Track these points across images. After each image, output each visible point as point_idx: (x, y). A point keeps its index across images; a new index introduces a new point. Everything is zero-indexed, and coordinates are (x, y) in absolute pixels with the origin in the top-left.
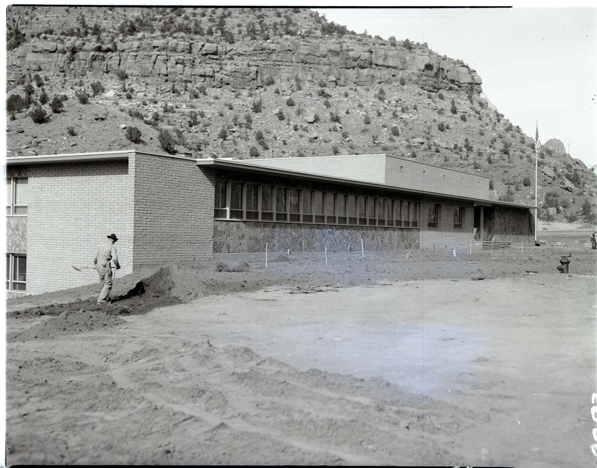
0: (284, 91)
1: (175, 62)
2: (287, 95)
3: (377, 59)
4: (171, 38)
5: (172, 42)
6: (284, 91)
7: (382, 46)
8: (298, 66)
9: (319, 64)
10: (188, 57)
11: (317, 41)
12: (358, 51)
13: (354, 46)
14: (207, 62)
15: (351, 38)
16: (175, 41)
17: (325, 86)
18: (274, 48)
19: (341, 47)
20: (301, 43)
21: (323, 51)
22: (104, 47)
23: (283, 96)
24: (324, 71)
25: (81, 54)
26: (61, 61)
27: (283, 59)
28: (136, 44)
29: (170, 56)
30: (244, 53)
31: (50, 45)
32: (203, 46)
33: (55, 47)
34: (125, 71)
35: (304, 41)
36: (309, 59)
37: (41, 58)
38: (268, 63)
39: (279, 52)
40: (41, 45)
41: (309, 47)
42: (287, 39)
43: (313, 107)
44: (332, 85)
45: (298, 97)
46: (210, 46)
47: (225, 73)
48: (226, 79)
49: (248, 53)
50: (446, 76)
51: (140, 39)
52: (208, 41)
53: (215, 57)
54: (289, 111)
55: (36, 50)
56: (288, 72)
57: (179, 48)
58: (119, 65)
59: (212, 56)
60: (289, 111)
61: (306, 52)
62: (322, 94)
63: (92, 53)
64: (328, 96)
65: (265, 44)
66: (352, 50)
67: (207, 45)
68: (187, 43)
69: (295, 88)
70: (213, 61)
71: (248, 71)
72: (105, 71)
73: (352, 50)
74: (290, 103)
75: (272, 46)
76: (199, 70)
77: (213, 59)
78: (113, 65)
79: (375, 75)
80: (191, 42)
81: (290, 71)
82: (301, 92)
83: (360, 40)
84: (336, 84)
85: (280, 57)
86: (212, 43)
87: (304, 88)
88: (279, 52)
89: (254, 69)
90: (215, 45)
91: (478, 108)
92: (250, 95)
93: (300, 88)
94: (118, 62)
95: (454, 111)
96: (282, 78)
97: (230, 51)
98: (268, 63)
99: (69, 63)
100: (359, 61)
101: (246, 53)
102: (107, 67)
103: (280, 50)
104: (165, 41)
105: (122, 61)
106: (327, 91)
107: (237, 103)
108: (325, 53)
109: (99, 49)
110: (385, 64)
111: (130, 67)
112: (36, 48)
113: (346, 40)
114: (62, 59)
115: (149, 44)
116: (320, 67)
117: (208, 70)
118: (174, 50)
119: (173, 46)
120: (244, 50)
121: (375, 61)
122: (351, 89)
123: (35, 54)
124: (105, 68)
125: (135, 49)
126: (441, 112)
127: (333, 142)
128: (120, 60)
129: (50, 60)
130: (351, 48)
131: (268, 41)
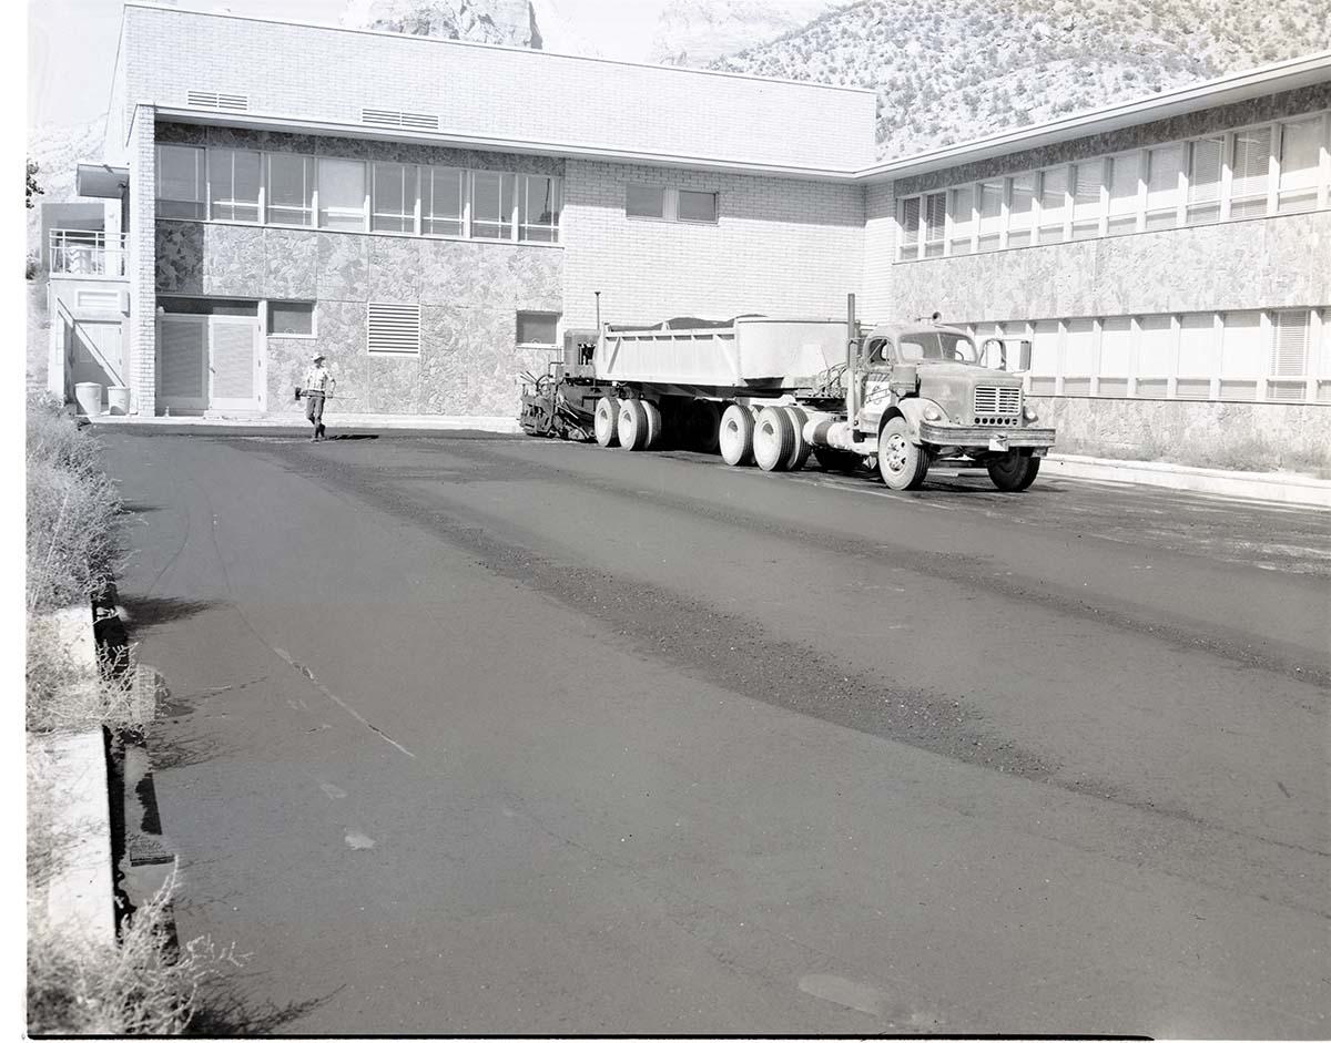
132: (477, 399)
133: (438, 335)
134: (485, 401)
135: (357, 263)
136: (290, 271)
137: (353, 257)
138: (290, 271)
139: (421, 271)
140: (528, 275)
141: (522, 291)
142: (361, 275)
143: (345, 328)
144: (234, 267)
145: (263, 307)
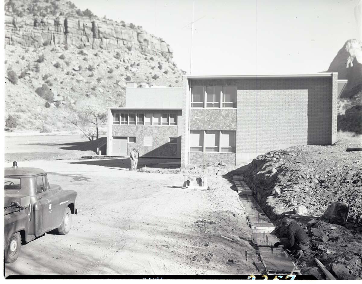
43: (76, 61)
45: (67, 54)
47: (18, 36)
50: (154, 47)
54: (61, 62)
60: (61, 62)
62: (81, 53)
64: (85, 54)
66: (101, 27)
73: (101, 27)
74: (62, 57)
91: (173, 67)
92: (35, 51)
95: (160, 67)
97: (21, 22)
106: (85, 51)
107: (27, 55)
122: (99, 51)
126: (153, 68)
127: (93, 83)
132: (162, 153)
133: (156, 142)
134: (163, 153)
135: (142, 130)
136: (131, 132)
137: (142, 129)
138: (131, 132)
139: (153, 131)
140: (171, 131)
141: (170, 134)
142: (143, 132)
143: (140, 141)
144: (124, 132)
145: (128, 138)
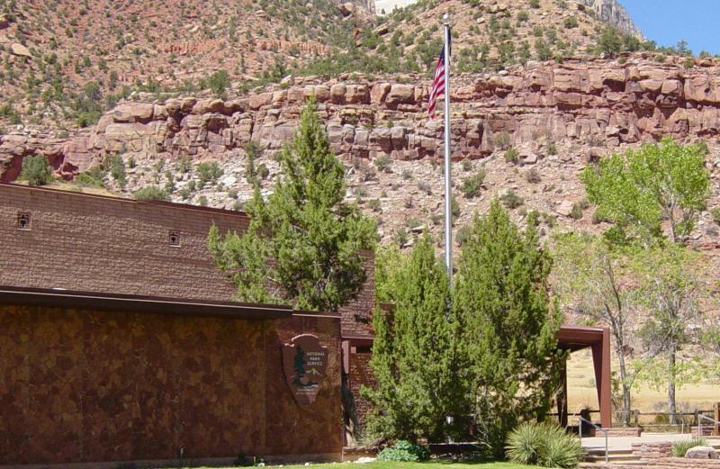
0: (525, 157)
1: (340, 120)
2: (528, 163)
3: (693, 91)
4: (335, 80)
5: (335, 86)
6: (525, 157)
7: (704, 69)
8: (552, 112)
9: (588, 106)
10: (361, 108)
11: (583, 66)
12: (659, 79)
13: (650, 69)
14: (397, 116)
15: (645, 57)
16: (342, 84)
17: (600, 144)
18: (510, 84)
19: (627, 73)
20: (556, 71)
21: (595, 83)
22: (229, 104)
23: (522, 165)
24: (598, 117)
25: (189, 120)
26: (159, 133)
27: (527, 103)
28: (277, 95)
29: (333, 111)
30: (459, 97)
31: (142, 110)
32: (388, 90)
33: (150, 111)
34: (259, 141)
35: (560, 67)
36: (572, 99)
37: (129, 130)
38: (500, 110)
39: (520, 90)
40: (126, 109)
41: (570, 77)
42: (532, 68)
44: (613, 142)
46: (400, 89)
47: (426, 132)
48: (427, 142)
49: (467, 96)
51: (284, 87)
52: (398, 81)
53: (410, 107)
55: (119, 118)
56: (535, 125)
57: (349, 95)
58: (251, 132)
59: (404, 106)
61: (565, 86)
63: (208, 115)
65: (493, 78)
66: (646, 77)
67: (395, 87)
68: (361, 87)
69: (544, 151)
70: (406, 114)
71: (463, 128)
72: (228, 144)
73: (646, 77)
74: (534, 179)
75: (507, 81)
76: (381, 131)
77: (406, 110)
78: (240, 134)
79: (691, 119)
80: (370, 84)
81: (539, 122)
82: (556, 157)
83: (661, 60)
84: (621, 141)
85: (520, 99)
86: (404, 83)
87: (560, 149)
88: (520, 90)
89: (476, 122)
90: (409, 86)
93: (553, 152)
94: (249, 127)
96: (525, 134)
98: (500, 110)
99: (171, 137)
100: (660, 97)
101: (463, 97)
102: (232, 138)
103: (520, 87)
104: (324, 86)
105: (256, 127)
108: (599, 86)
109: (219, 108)
110: (708, 99)
111: (267, 134)
112: (120, 114)
113: (636, 61)
114: (158, 129)
115: (300, 93)
116: (590, 111)
117: (396, 131)
118: (340, 100)
119: (338, 93)
120: (460, 90)
121: (689, 94)
123: (119, 125)
124: (229, 139)
125: (275, 104)
128: (253, 125)
129: (142, 132)
130: (643, 73)
131: (501, 72)
